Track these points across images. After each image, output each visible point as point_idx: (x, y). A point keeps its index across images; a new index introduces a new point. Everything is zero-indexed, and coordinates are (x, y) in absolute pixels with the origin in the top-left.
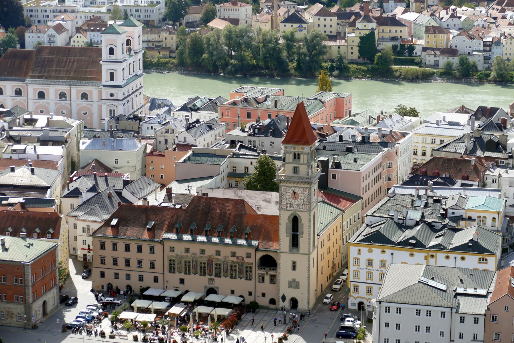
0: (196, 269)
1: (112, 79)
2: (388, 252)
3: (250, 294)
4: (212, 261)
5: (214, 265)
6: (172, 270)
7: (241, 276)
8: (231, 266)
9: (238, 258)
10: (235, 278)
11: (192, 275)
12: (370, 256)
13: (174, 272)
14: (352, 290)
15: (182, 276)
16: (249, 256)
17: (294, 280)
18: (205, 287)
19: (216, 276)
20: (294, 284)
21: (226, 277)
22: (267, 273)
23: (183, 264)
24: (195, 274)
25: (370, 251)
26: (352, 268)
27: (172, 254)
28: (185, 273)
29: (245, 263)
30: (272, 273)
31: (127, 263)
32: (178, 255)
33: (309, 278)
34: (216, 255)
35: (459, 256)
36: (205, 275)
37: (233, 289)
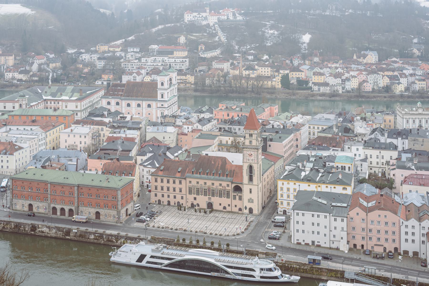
1: (162, 97)
2: (297, 184)
3: (229, 205)
6: (190, 193)
9: (223, 187)
10: (221, 197)
11: (200, 195)
12: (288, 186)
13: (191, 194)
14: (280, 204)
15: (195, 196)
16: (228, 185)
17: (251, 199)
18: (207, 202)
19: (212, 196)
20: (251, 201)
22: (237, 195)
23: (196, 190)
25: (288, 183)
26: (279, 193)
27: (190, 184)
28: (197, 195)
29: (226, 189)
30: (240, 195)
31: (168, 189)
33: (258, 197)
35: (333, 186)
36: (206, 195)
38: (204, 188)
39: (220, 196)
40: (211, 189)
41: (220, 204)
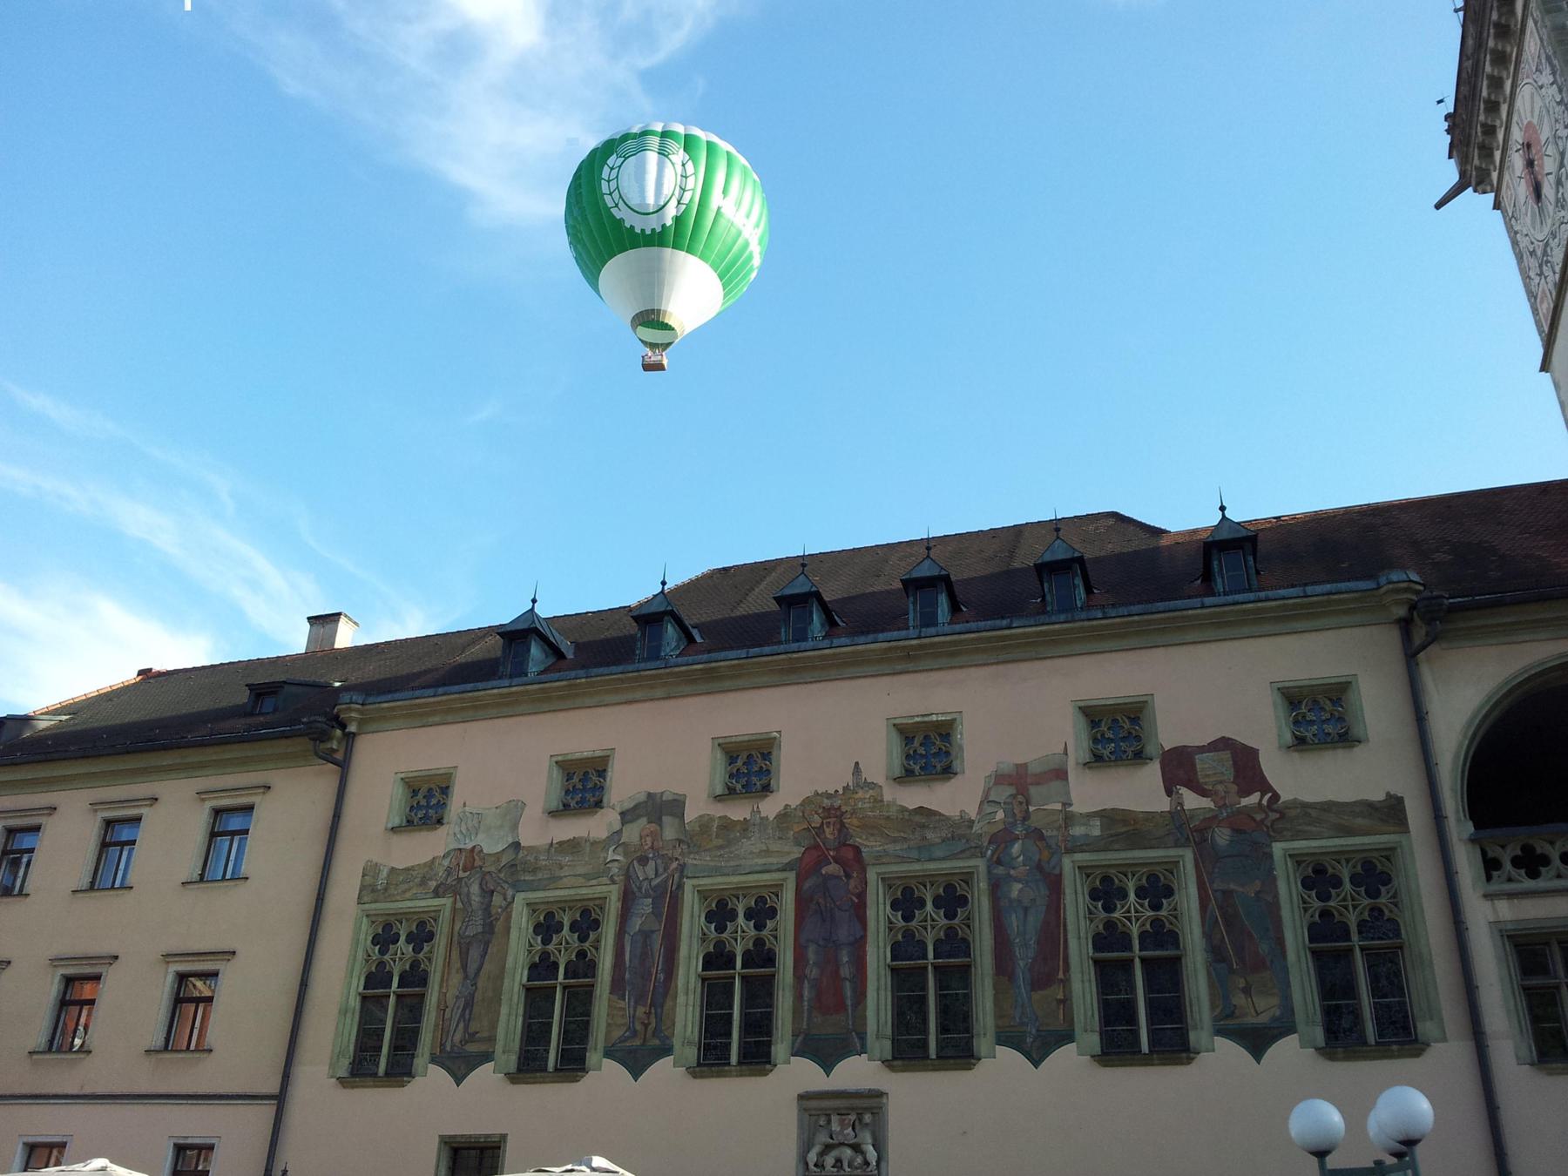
0: (660, 995)
4: (854, 861)
5: (878, 911)
7: (1263, 1009)
8: (1105, 892)
10: (1173, 1045)
16: (1319, 716)
19: (907, 1052)
21: (1038, 1046)
23: (518, 948)
24: (636, 1063)
32: (470, 859)
34: (907, 776)
36: (757, 1057)
39: (1143, 1021)
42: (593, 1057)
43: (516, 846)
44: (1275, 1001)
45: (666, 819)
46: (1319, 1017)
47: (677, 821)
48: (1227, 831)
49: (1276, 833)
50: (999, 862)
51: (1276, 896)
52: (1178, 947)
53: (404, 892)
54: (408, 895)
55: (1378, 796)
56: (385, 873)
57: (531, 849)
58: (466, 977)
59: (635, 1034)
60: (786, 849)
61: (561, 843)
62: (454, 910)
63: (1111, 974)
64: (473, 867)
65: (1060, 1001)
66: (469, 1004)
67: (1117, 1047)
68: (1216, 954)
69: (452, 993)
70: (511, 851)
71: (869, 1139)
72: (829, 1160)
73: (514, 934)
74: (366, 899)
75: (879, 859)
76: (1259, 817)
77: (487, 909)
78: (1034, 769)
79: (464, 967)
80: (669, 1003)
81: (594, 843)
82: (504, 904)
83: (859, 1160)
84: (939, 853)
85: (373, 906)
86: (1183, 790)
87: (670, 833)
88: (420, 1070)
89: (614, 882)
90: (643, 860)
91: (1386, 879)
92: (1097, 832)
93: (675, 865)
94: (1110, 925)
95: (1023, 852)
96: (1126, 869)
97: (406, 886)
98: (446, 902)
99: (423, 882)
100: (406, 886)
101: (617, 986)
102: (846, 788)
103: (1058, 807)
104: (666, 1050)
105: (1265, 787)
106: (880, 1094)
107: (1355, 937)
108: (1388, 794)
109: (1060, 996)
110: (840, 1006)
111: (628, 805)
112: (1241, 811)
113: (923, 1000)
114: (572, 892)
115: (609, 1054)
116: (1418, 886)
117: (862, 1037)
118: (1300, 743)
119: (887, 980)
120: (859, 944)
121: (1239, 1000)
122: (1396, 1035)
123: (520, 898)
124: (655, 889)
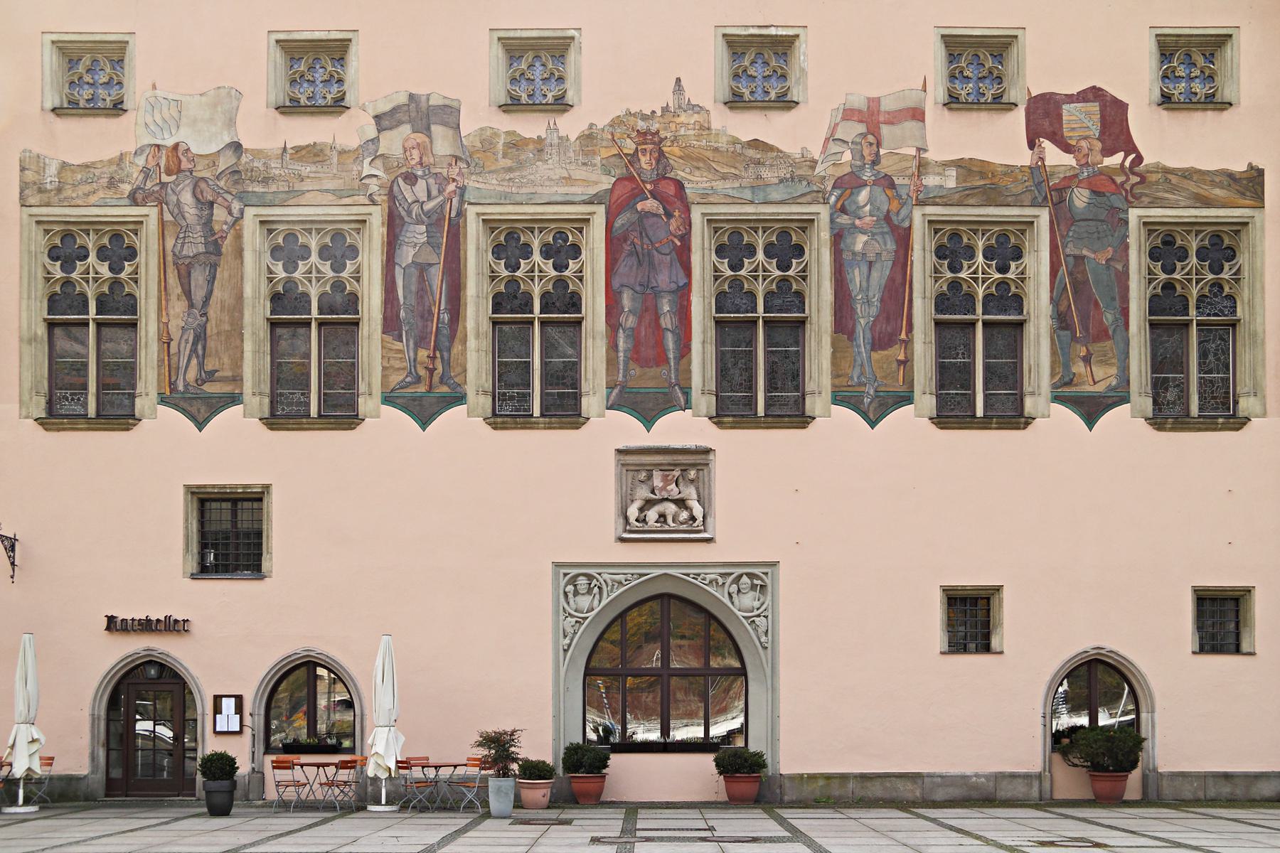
5: (702, 258)
7: (1101, 378)
8: (951, 250)
9: (1044, 117)
10: (1010, 415)
11: (384, 424)
13: (116, 414)
15: (237, 449)
18: (575, 578)
19: (733, 410)
23: (254, 273)
27: (92, 141)
29: (1143, 182)
34: (735, 102)
36: (564, 409)
37: (970, 578)
38: (488, 199)
40: (713, 198)
41: (971, 619)
42: (365, 405)
43: (236, 147)
44: (1114, 371)
45: (437, 130)
46: (1149, 389)
47: (451, 132)
48: (1086, 193)
49: (1133, 198)
50: (843, 210)
51: (1126, 266)
52: (1021, 313)
53: (87, 195)
54: (93, 199)
55: (1239, 167)
56: (52, 170)
57: (257, 153)
58: (191, 306)
59: (418, 380)
60: (593, 177)
61: (298, 149)
62: (162, 224)
63: (951, 333)
64: (179, 171)
65: (900, 363)
66: (201, 337)
67: (952, 414)
68: (1061, 320)
69: (175, 325)
70: (229, 153)
71: (695, 496)
72: (652, 515)
73: (248, 256)
74: (32, 201)
75: (705, 199)
76: (1119, 180)
77: (208, 223)
78: (888, 105)
79: (188, 293)
80: (457, 348)
81: (342, 153)
82: (230, 219)
83: (684, 515)
84: (775, 196)
85: (44, 210)
86: (1047, 144)
87: (442, 144)
88: (147, 412)
89: (374, 203)
90: (411, 179)
91: (1231, 254)
92: (951, 183)
93: (451, 187)
94: (955, 285)
95: (870, 200)
96: (977, 226)
97: (87, 188)
98: (151, 212)
99: (112, 184)
100: (87, 188)
101: (391, 324)
102: (665, 110)
103: (913, 152)
104: (460, 399)
105: (1130, 147)
106: (707, 451)
107: (1193, 312)
108: (1250, 164)
109: (901, 357)
110: (662, 359)
111: (385, 107)
112: (1101, 172)
113: (751, 356)
114: (320, 210)
115: (388, 400)
116: (1263, 264)
117: (687, 392)
118: (1166, 100)
119: (712, 333)
120: (683, 294)
121: (1079, 368)
122: (1216, 409)
123: (250, 212)
124: (428, 214)
